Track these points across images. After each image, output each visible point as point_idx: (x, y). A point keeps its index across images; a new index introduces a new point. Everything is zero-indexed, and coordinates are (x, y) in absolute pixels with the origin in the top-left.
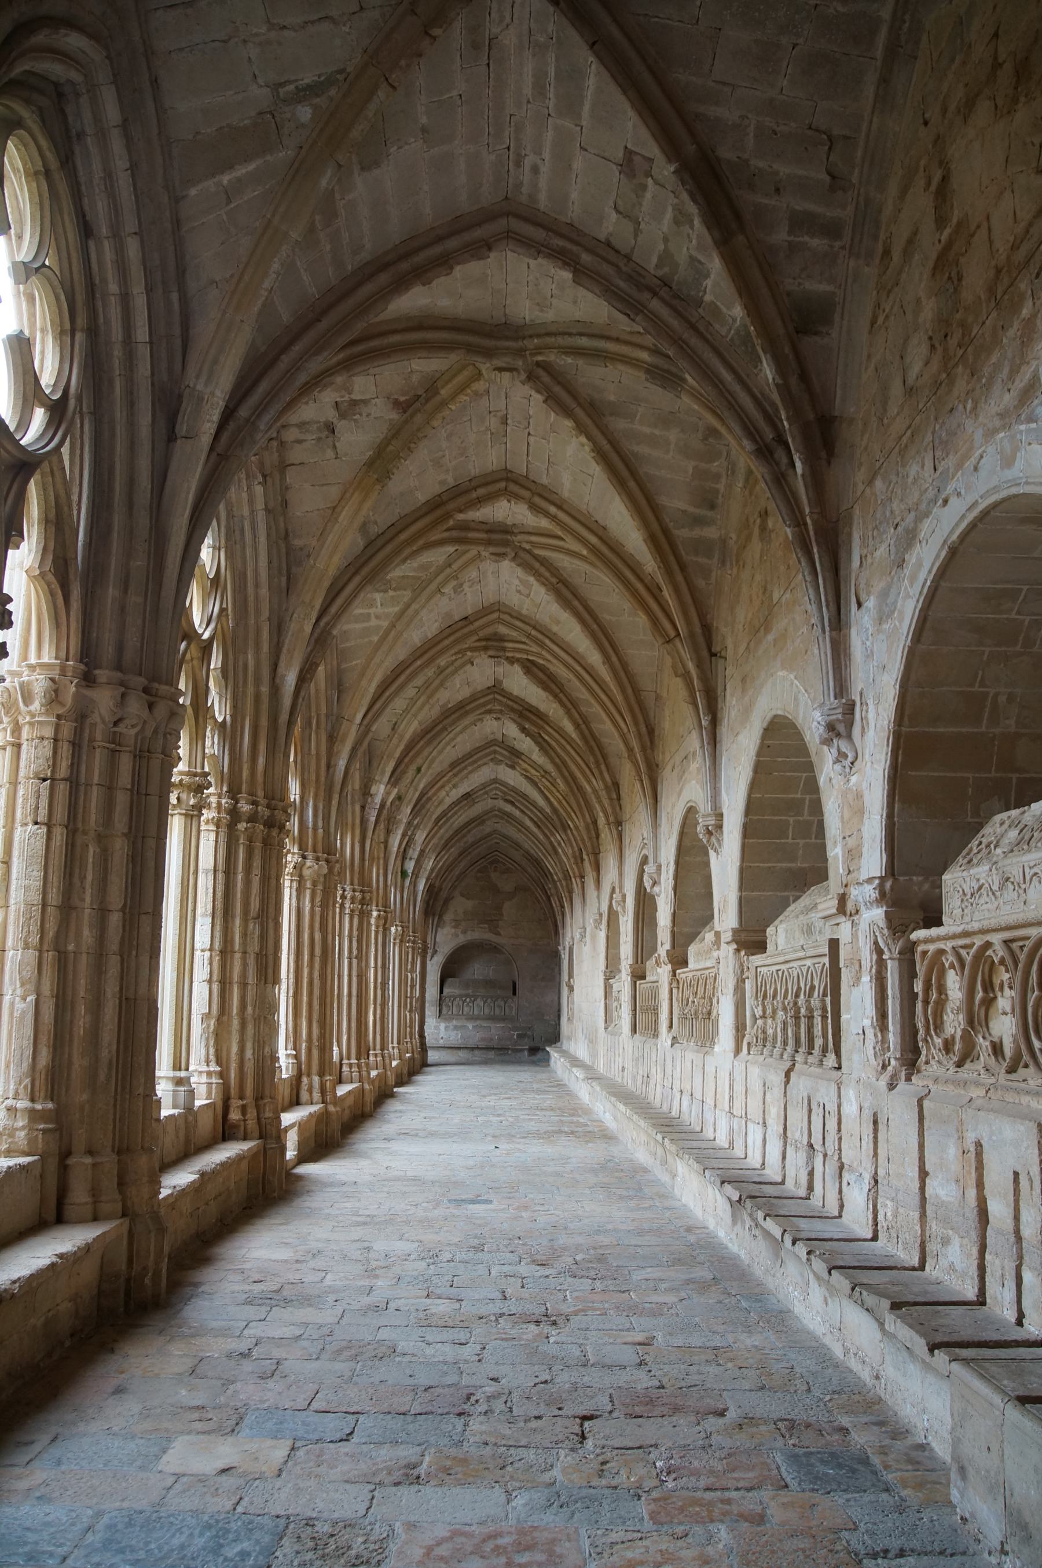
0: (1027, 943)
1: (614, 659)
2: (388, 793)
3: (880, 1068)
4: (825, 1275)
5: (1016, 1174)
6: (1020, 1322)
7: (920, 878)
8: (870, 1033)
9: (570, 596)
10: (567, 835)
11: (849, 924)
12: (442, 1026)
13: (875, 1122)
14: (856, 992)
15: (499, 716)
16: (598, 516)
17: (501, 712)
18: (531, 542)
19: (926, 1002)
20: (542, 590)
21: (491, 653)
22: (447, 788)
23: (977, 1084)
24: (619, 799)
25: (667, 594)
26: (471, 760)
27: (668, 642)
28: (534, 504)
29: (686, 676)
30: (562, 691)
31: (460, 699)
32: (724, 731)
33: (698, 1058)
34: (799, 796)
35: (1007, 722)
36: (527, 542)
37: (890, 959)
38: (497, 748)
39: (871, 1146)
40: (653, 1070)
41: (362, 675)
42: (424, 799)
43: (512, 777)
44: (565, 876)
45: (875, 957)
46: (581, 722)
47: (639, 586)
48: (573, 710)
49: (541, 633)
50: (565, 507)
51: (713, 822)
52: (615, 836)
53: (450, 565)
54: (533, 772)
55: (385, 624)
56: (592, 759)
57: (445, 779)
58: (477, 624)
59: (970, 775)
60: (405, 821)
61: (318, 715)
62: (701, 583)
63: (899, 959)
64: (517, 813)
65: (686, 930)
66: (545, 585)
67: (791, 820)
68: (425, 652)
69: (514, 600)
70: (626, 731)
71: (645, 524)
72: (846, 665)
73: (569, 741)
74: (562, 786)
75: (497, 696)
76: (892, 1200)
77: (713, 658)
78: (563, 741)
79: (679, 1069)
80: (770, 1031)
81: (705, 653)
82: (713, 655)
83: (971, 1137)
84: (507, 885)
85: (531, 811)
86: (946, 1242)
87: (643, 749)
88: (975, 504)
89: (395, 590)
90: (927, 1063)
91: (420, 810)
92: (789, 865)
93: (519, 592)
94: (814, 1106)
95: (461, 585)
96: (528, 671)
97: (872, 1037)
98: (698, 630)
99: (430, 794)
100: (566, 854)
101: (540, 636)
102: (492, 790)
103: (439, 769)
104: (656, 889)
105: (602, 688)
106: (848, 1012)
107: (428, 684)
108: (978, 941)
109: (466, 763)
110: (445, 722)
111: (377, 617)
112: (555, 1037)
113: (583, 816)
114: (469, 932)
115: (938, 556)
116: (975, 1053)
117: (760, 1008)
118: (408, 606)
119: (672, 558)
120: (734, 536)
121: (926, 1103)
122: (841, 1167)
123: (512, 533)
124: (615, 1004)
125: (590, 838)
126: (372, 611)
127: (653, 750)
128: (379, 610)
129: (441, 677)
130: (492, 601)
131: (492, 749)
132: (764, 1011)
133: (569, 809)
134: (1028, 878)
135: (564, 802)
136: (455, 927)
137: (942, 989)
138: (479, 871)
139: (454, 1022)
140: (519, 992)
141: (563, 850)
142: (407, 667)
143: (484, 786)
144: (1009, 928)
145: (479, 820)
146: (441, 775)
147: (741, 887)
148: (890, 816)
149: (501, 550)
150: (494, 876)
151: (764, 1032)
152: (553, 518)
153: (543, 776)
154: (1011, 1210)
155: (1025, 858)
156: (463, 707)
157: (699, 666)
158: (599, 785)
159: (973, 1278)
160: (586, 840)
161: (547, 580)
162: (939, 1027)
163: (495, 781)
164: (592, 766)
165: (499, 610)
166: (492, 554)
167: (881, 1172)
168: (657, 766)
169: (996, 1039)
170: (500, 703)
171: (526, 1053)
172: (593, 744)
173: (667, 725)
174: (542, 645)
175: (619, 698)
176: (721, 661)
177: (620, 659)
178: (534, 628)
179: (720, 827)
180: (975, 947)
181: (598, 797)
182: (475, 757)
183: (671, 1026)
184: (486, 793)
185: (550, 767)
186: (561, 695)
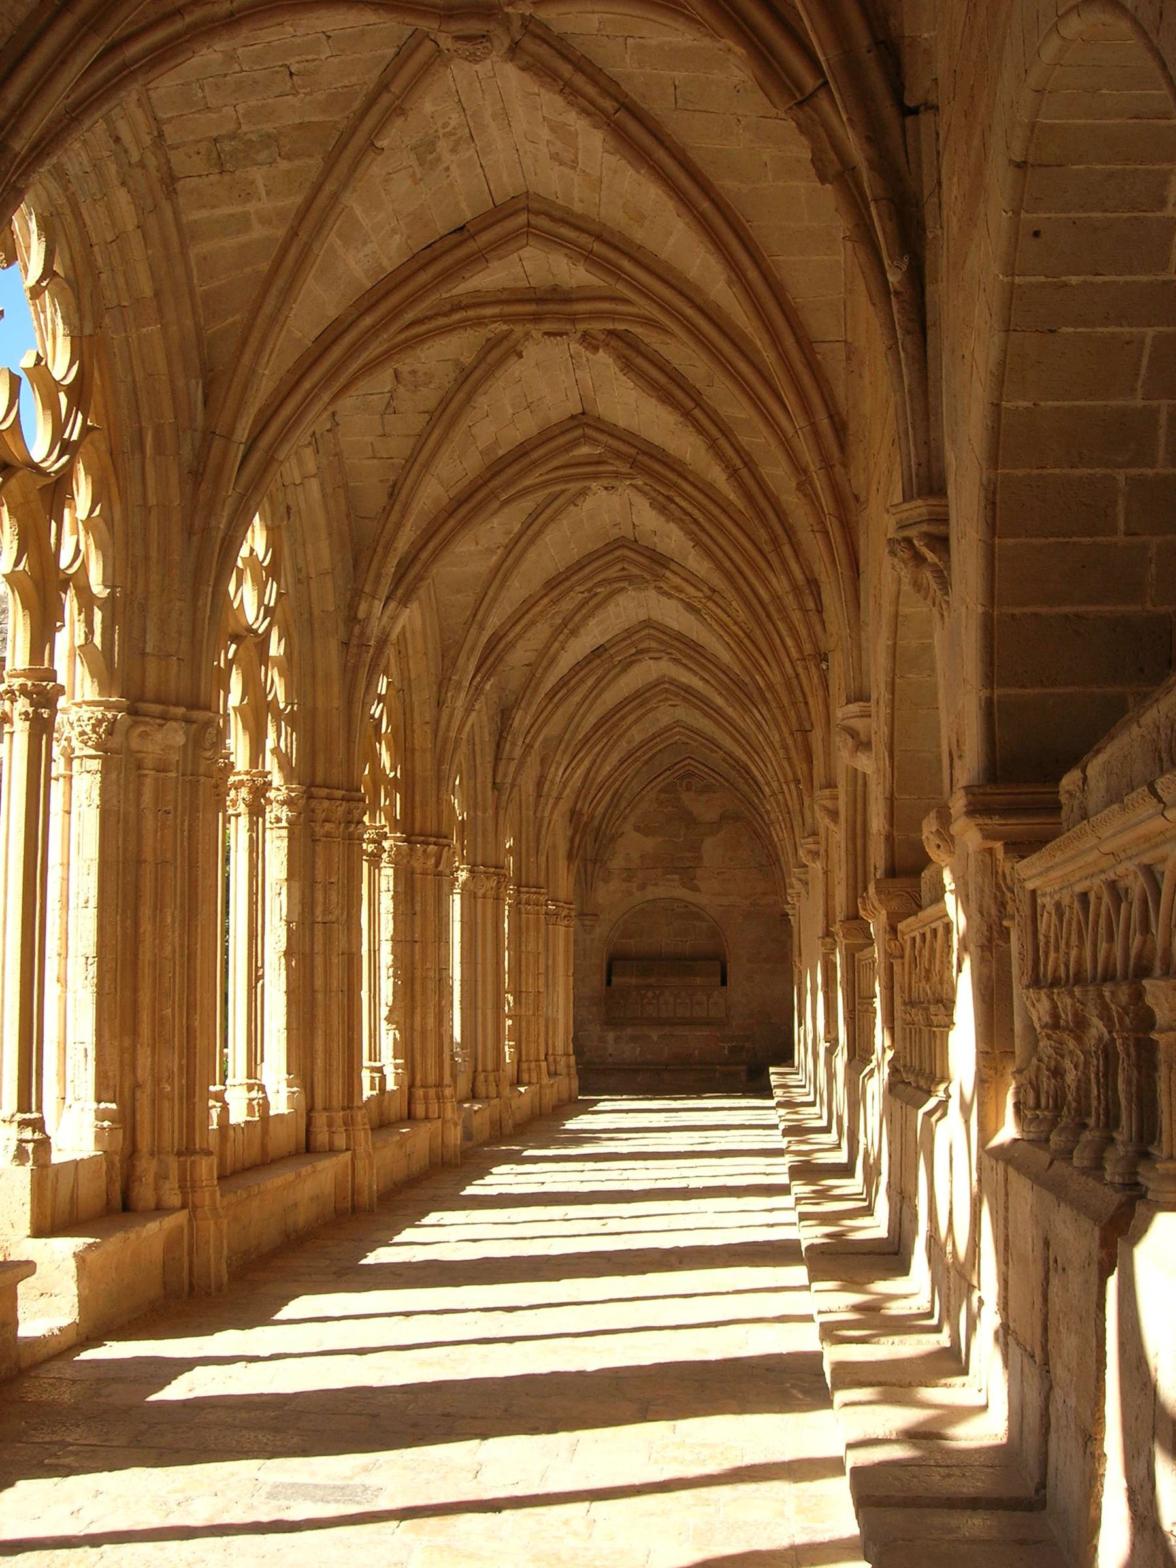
1: (753, 274)
12: (611, 1036)
17: (617, 475)
21: (547, 326)
22: (562, 637)
24: (820, 611)
26: (581, 574)
27: (800, 104)
30: (698, 405)
31: (520, 438)
34: (1138, 402)
38: (627, 552)
41: (244, 343)
42: (501, 646)
46: (738, 463)
48: (723, 442)
51: (925, 528)
54: (691, 591)
55: (281, 232)
56: (762, 535)
57: (537, 609)
58: (485, 238)
61: (158, 431)
66: (589, 114)
67: (1120, 476)
70: (790, 431)
74: (743, 615)
75: (589, 432)
77: (909, 121)
78: (716, 511)
81: (888, 111)
82: (908, 112)
84: (705, 810)
87: (827, 465)
89: (289, 158)
91: (494, 666)
93: (555, 157)
95: (431, 146)
96: (628, 366)
99: (511, 635)
100: (771, 744)
101: (612, 255)
102: (641, 640)
103: (525, 593)
107: (444, 403)
109: (574, 579)
110: (493, 484)
111: (264, 221)
114: (650, 889)
118: (318, 188)
125: (794, 704)
126: (250, 207)
127: (845, 466)
128: (265, 204)
129: (467, 387)
131: (618, 553)
133: (756, 654)
136: (627, 880)
138: (662, 791)
139: (629, 1031)
140: (731, 979)
141: (766, 737)
143: (629, 633)
145: (640, 698)
146: (529, 604)
149: (475, 26)
150: (686, 797)
153: (709, 598)
156: (526, 454)
157: (874, 136)
158: (781, 584)
161: (592, 103)
163: (648, 624)
164: (767, 548)
165: (528, 210)
168: (856, 498)
172: (764, 504)
175: (769, 356)
176: (925, 118)
177: (765, 275)
178: (598, 238)
181: (782, 609)
184: (633, 644)
185: (717, 580)
186: (697, 412)
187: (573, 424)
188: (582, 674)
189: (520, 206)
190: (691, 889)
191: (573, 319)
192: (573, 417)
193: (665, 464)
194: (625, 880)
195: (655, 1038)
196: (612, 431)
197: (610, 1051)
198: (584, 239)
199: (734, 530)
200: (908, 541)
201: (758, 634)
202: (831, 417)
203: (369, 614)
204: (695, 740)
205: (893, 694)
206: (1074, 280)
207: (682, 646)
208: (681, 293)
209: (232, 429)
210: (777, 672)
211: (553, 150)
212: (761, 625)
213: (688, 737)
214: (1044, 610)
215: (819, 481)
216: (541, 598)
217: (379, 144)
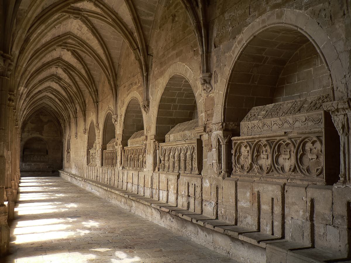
0: (276, 141)
1: (107, 52)
2: (24, 90)
3: (218, 174)
4: (213, 229)
5: (273, 199)
6: (273, 234)
7: (232, 123)
8: (215, 165)
9: (95, 32)
10: (72, 105)
11: (207, 135)
12: (24, 164)
13: (217, 188)
14: (209, 154)
15: (58, 67)
16: (116, 10)
18: (88, 15)
19: (235, 156)
20: (86, 28)
21: (62, 47)
23: (256, 177)
24: (98, 95)
25: (136, 34)
27: (134, 50)
28: (96, 4)
29: (139, 60)
31: (48, 61)
32: (151, 77)
33: (136, 173)
34: (175, 98)
35: (255, 82)
36: (86, 14)
37: (223, 144)
38: (54, 77)
39: (215, 194)
40: (113, 176)
42: (30, 92)
43: (55, 86)
44: (68, 117)
45: (217, 144)
46: (87, 70)
47: (127, 32)
48: (85, 67)
49: (83, 43)
50: (105, 5)
51: (147, 104)
52: (96, 106)
53: (59, 19)
56: (90, 82)
57: (37, 86)
58: (63, 38)
59: (245, 96)
60: (24, 99)
62: (146, 33)
63: (226, 145)
64: (53, 97)
65: (127, 135)
67: (172, 104)
68: (46, 46)
69: (75, 32)
71: (133, 14)
72: (209, 63)
73: (83, 76)
75: (60, 61)
76: (224, 208)
77: (148, 56)
78: (81, 76)
79: (126, 176)
80: (167, 165)
81: (146, 54)
83: (256, 190)
84: (45, 119)
85: (61, 97)
86: (246, 217)
87: (114, 80)
88: (266, 26)
90: (235, 172)
92: (171, 117)
93: (78, 29)
94: (190, 185)
96: (73, 54)
97: (216, 165)
98: (145, 47)
99: (32, 90)
102: (48, 90)
104: (116, 123)
105: (101, 61)
106: (206, 158)
108: (257, 141)
109: (44, 81)
110: (43, 68)
112: (61, 167)
113: (81, 99)
115: (250, 38)
116: (253, 169)
117: (163, 158)
119: (139, 25)
120: (159, 21)
121: (238, 182)
122: (202, 200)
123: (81, 11)
124: (91, 157)
125: (83, 106)
130: (68, 31)
131: (52, 77)
132: (164, 159)
133: (76, 97)
134: (273, 124)
135: (75, 95)
137: (240, 152)
139: (28, 163)
142: (40, 50)
143: (46, 88)
144: (268, 137)
145: (41, 99)
147: (157, 124)
148: (225, 106)
150: (41, 117)
151: (164, 165)
152: (102, 9)
153: (69, 86)
154: (271, 208)
155: (272, 119)
156: (49, 63)
157: (144, 58)
159: (255, 226)
160: (82, 107)
161: (89, 26)
162: (239, 163)
163: (49, 87)
165: (70, 34)
166: (74, 17)
167: (219, 201)
168: (117, 86)
169: (261, 165)
170: (61, 63)
171: (51, 172)
173: (122, 73)
174: (83, 46)
175: (107, 64)
176: (151, 57)
178: (81, 41)
179: (148, 106)
180: (256, 142)
182: (47, 79)
183: (121, 164)
185: (72, 84)
186: (82, 62)
187: (57, 59)
188: (36, 95)
189: (69, 33)
190: (41, 135)
191: (67, 46)
192: (57, 58)
193: (73, 68)
194: (28, 133)
195: (33, 165)
196: (64, 61)
197: (24, 167)
198: (79, 41)
199: (83, 80)
200: (145, 105)
201: (78, 94)
202: (115, 74)
203: (21, 89)
204: (47, 106)
205: (125, 116)
206: (172, 87)
207: (55, 92)
208: (93, 51)
209: (23, 65)
210: (80, 100)
211: (78, 28)
212: (79, 92)
213: (46, 106)
214: (163, 117)
215: (112, 83)
216: (38, 84)
217: (56, 27)
